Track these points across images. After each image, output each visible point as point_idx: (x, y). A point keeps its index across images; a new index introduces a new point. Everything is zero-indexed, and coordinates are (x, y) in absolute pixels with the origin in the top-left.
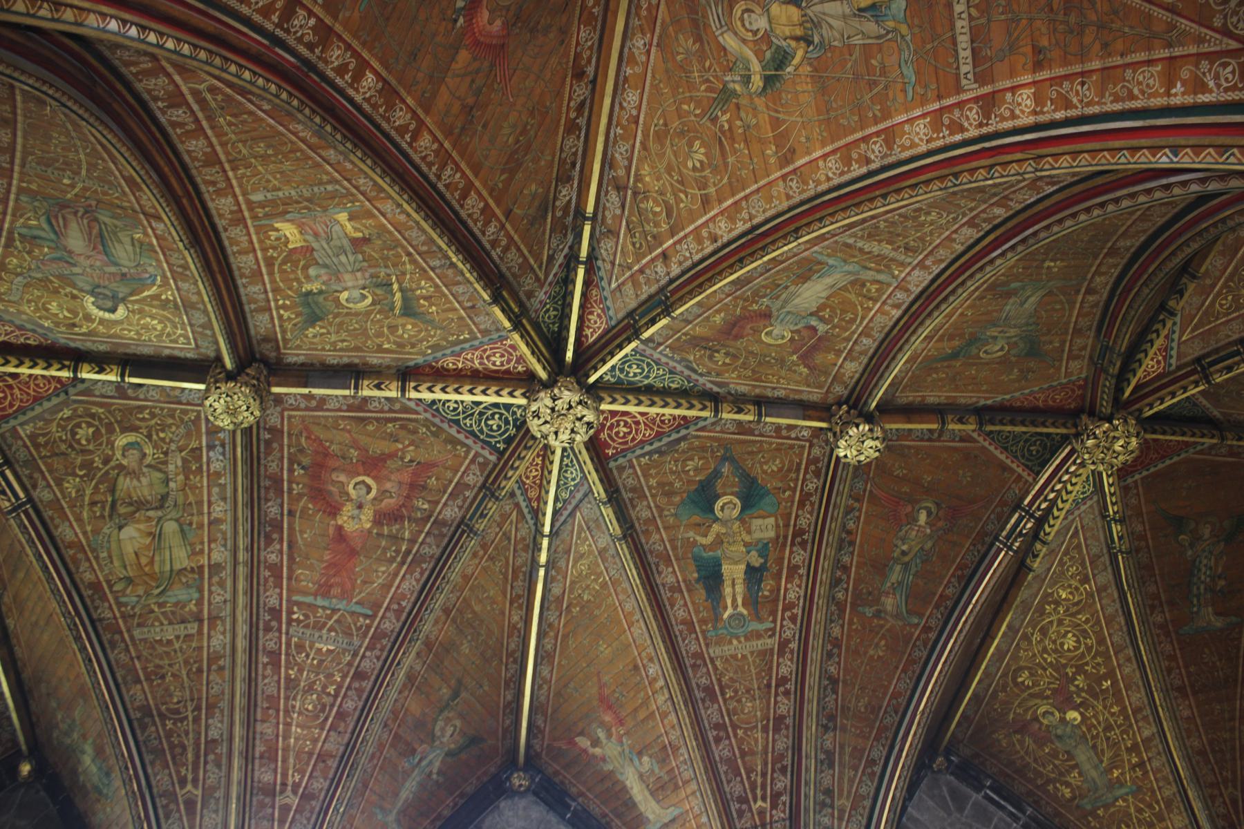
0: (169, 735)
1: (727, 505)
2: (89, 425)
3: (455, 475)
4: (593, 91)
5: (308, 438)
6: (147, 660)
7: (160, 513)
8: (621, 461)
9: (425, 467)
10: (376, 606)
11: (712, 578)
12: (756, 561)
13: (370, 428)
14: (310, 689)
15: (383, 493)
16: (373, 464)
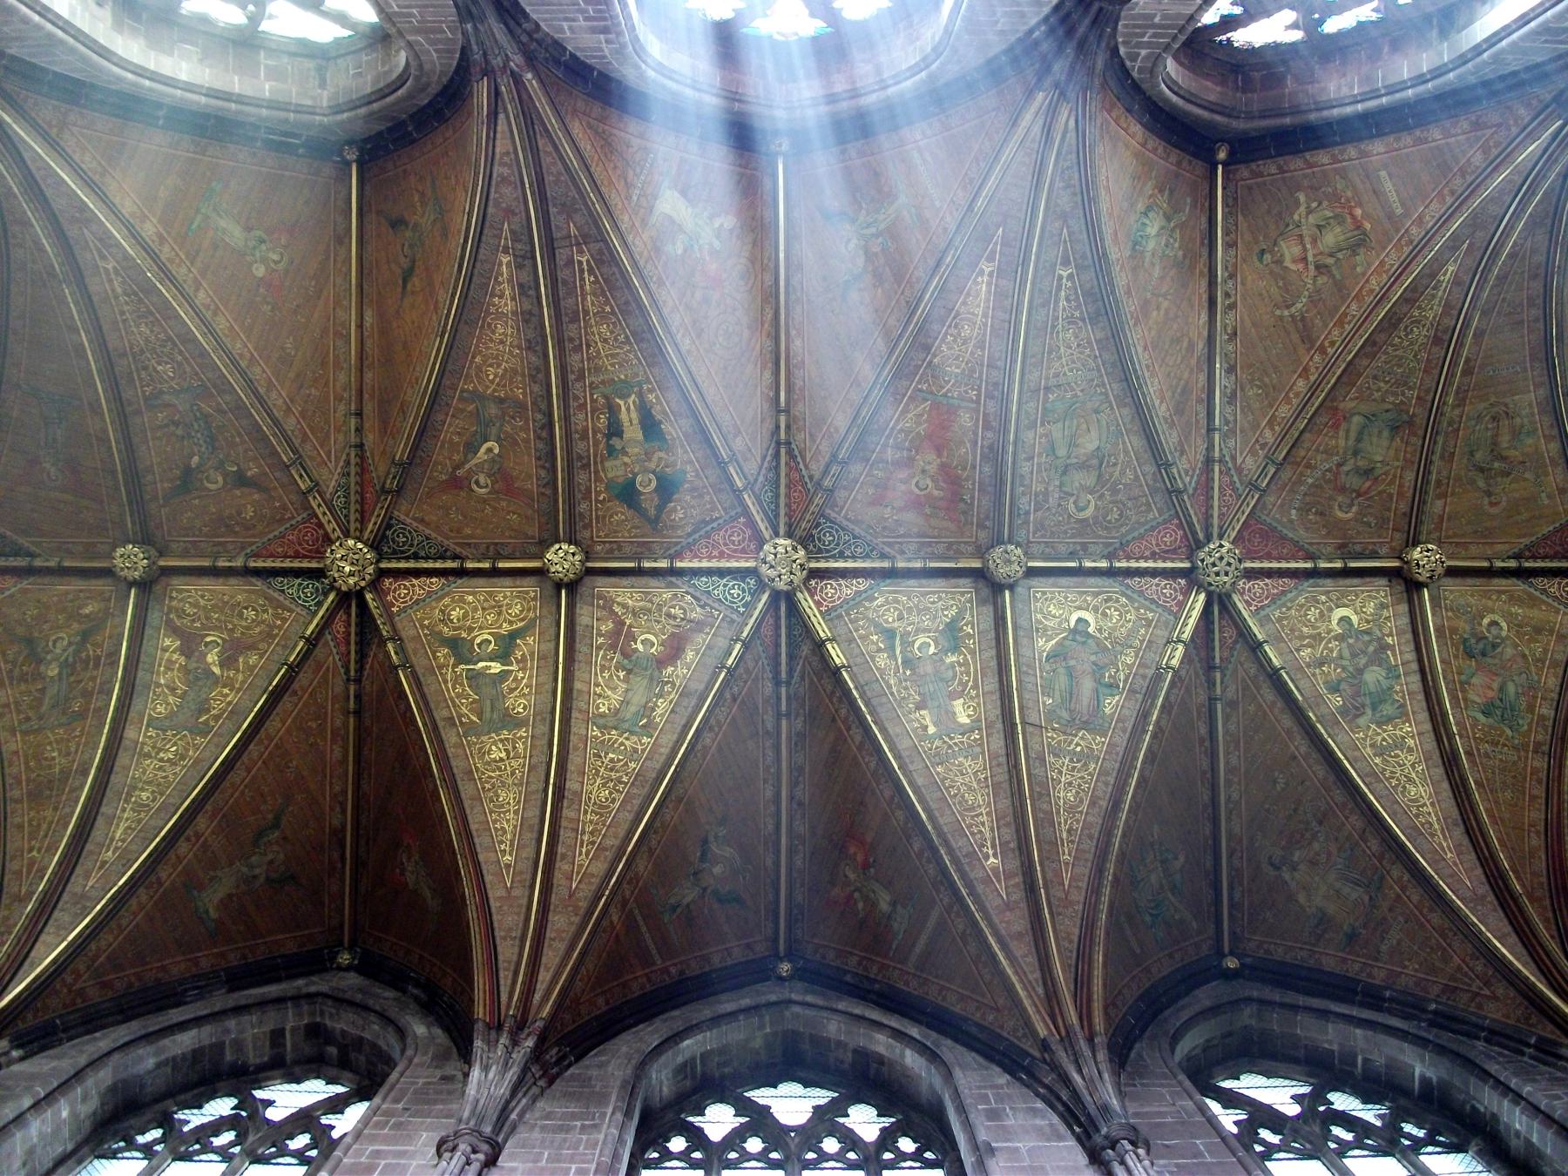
0: (1078, 307)
2: (1110, 522)
8: (733, 513)
9: (877, 501)
12: (615, 441)
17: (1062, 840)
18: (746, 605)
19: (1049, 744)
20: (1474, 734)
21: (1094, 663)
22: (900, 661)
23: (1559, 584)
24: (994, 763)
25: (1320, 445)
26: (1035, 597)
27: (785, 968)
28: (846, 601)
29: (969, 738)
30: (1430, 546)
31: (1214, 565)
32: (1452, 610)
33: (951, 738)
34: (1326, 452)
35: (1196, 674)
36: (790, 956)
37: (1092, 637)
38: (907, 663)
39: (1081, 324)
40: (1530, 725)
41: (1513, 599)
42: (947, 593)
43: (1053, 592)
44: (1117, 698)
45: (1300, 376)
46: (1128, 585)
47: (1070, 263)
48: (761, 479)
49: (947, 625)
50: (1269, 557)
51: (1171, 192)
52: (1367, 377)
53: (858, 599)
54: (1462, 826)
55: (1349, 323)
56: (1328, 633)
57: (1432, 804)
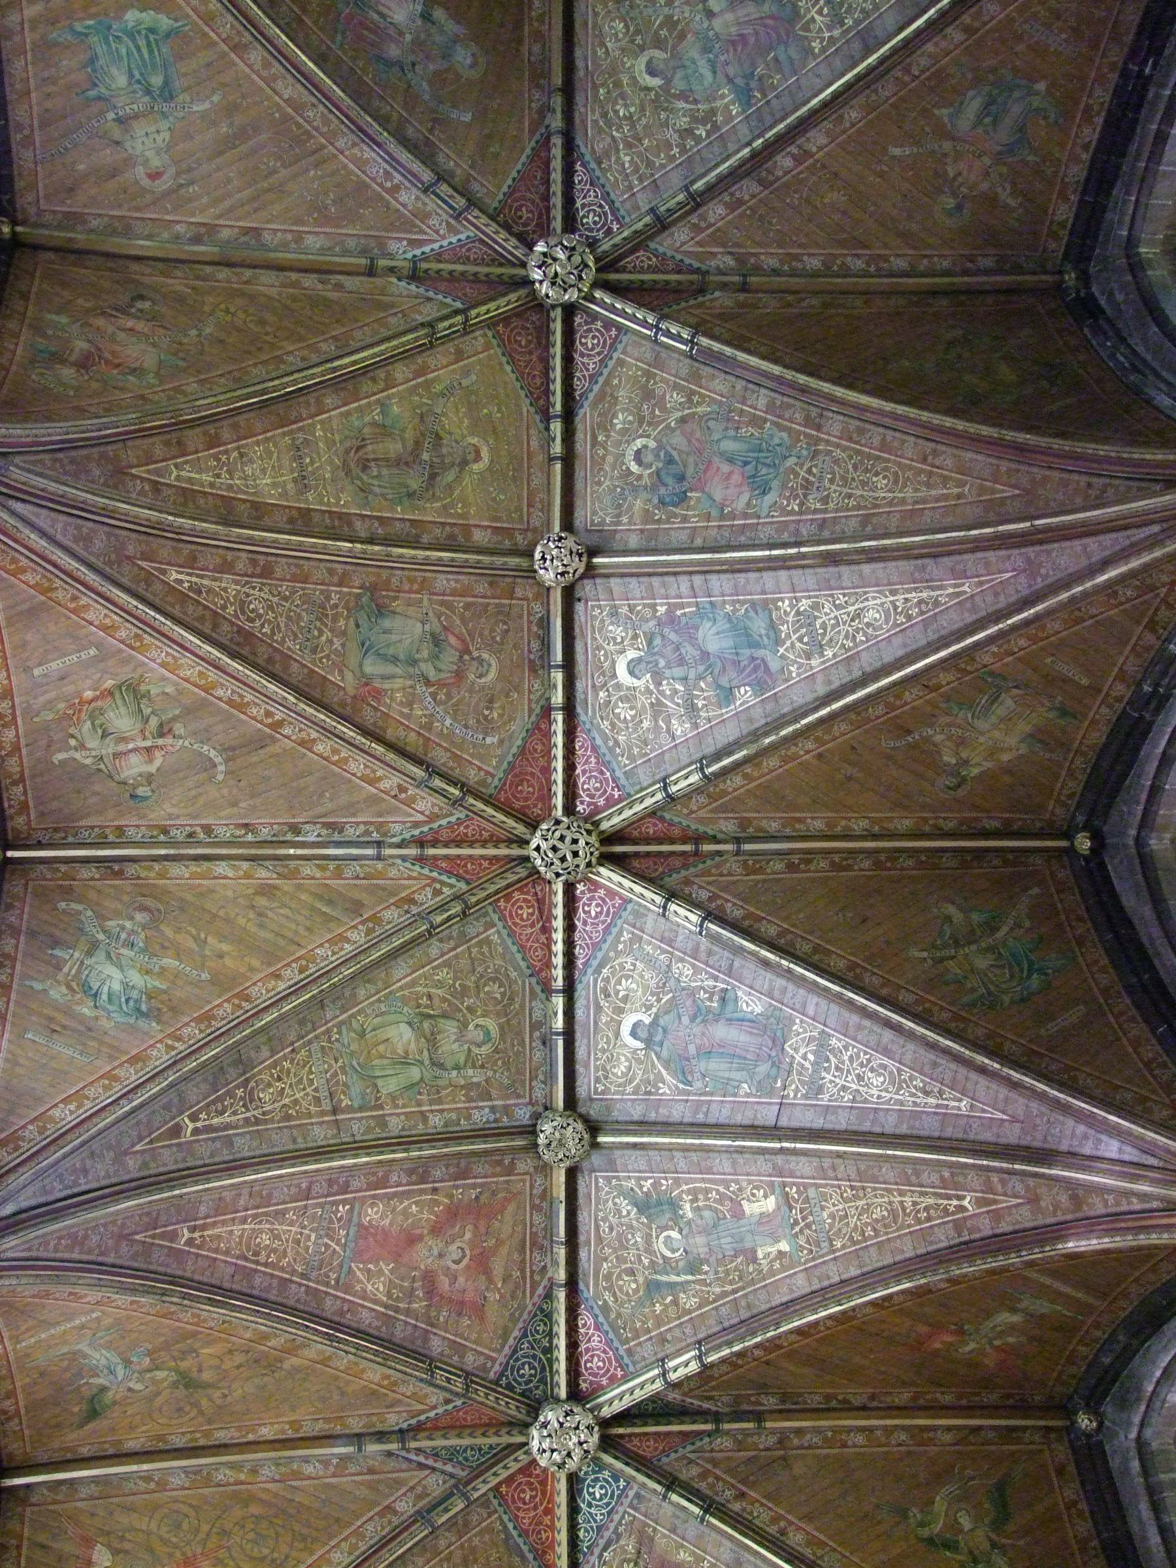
0: (230, 1094)
2: (503, 994)
3: (474, 1342)
4: (858, 1409)
5: (505, 1198)
6: (292, 1060)
7: (427, 1062)
8: (496, 1502)
9: (479, 1310)
10: (348, 1289)
13: (516, 1256)
16: (481, 1263)
17: (937, 1106)
18: (616, 1478)
19: (806, 1097)
20: (792, 512)
21: (693, 1019)
22: (690, 1278)
23: (582, 355)
24: (831, 1174)
25: (402, 714)
26: (603, 1093)
27: (1085, 1422)
28: (609, 1343)
29: (797, 1201)
30: (537, 556)
31: (563, 859)
32: (619, 515)
33: (796, 1223)
34: (410, 704)
35: (704, 874)
37: (657, 1016)
38: (693, 1269)
39: (252, 1084)
40: (782, 428)
41: (605, 425)
42: (597, 1210)
43: (597, 1069)
44: (740, 994)
45: (310, 750)
46: (585, 964)
47: (177, 1125)
48: (449, 1468)
49: (641, 1211)
50: (547, 771)
51: (56, 943)
52: (313, 662)
53: (606, 1327)
54: (927, 561)
55: (242, 697)
56: (651, 693)
57: (893, 593)
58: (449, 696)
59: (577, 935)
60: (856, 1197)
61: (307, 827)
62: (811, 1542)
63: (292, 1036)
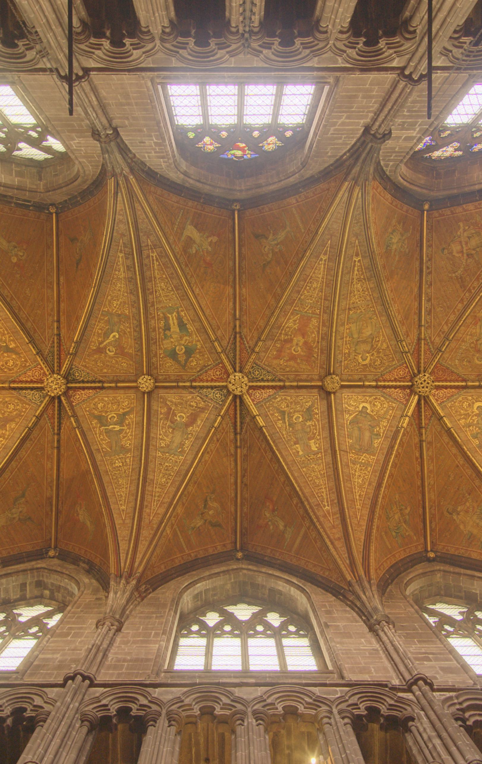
0: (363, 274)
1: (181, 350)
9: (278, 357)
10: (292, 314)
11: (182, 325)
12: (167, 332)
14: (314, 289)
15: (290, 349)
16: (293, 358)
21: (370, 425)
27: (240, 555)
31: (422, 383)
34: (471, 335)
35: (414, 430)
36: (242, 549)
38: (290, 425)
48: (229, 348)
49: (307, 409)
58: (472, 348)
59: (393, 389)
60: (321, 474)
61: (430, 304)
62: (206, 461)
63: (375, 295)
